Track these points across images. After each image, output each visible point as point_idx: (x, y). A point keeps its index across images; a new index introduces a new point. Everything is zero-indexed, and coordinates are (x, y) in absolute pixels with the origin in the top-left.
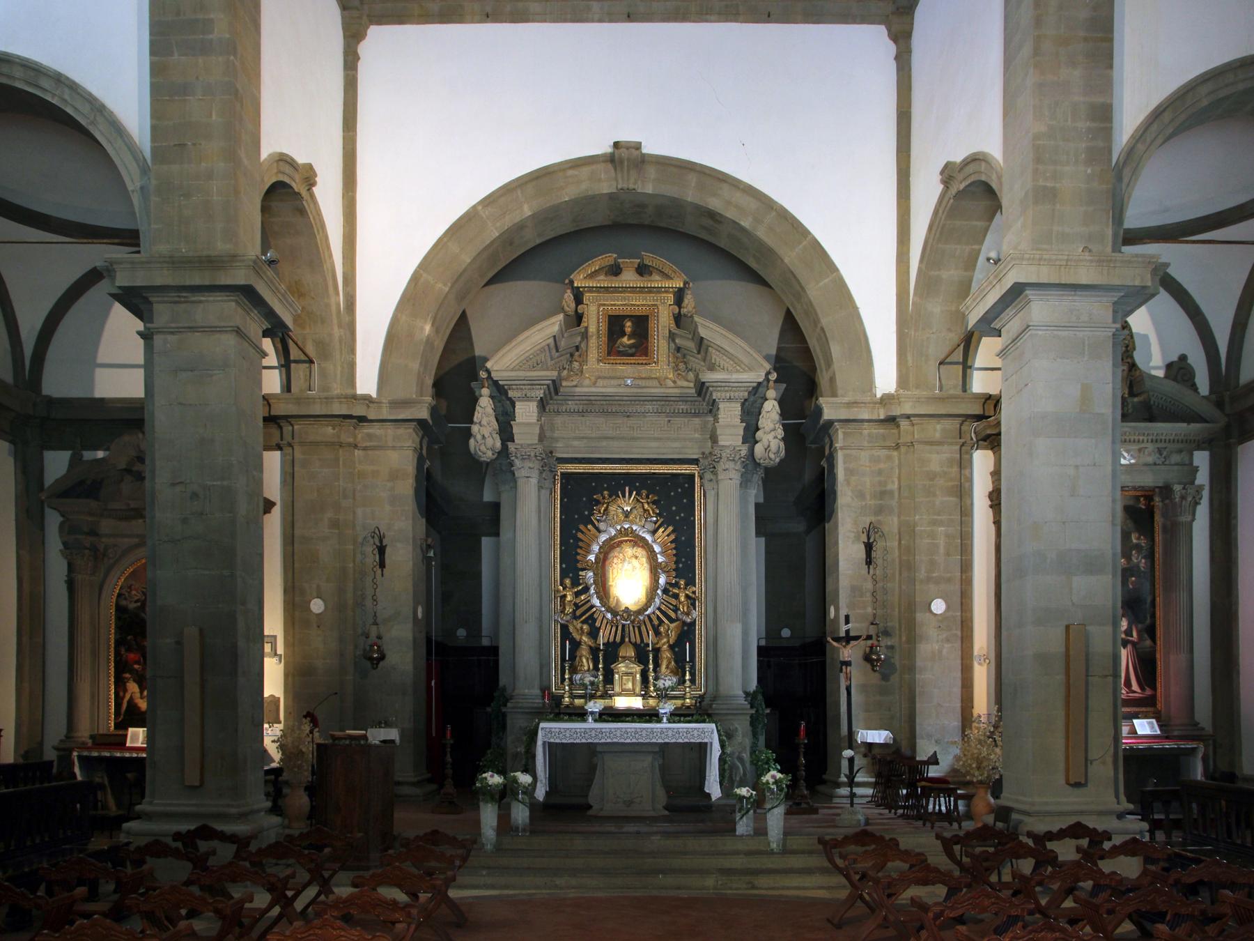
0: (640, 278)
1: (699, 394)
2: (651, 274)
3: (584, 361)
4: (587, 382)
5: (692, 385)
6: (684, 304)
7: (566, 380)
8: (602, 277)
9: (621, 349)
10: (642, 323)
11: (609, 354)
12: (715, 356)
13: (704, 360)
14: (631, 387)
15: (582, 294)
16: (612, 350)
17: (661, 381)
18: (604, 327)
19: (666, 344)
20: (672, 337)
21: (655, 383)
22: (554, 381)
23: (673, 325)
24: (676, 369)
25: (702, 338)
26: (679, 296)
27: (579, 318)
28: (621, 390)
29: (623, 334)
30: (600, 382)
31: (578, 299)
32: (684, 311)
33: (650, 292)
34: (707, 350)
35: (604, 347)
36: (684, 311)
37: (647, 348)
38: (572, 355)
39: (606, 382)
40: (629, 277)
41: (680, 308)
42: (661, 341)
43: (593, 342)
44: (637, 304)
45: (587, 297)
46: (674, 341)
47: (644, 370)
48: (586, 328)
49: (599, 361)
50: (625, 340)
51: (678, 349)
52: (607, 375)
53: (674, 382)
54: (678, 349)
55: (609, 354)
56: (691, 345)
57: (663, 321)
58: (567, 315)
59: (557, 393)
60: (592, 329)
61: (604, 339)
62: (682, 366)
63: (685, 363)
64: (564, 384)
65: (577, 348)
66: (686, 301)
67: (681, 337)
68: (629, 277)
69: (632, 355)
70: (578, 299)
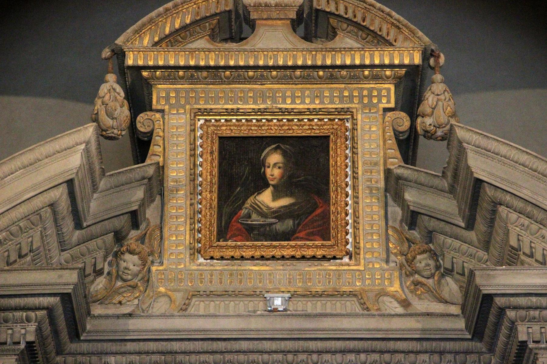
0: (306, 45)
1: (477, 332)
2: (332, 34)
3: (152, 254)
4: (161, 306)
5: (455, 310)
6: (426, 107)
7: (101, 301)
8: (202, 43)
9: (256, 220)
10: (310, 160)
11: (222, 234)
12: (517, 229)
13: (486, 245)
14: (285, 314)
15: (147, 85)
16: (231, 220)
17: (366, 302)
18: (208, 168)
19: (377, 209)
20: (394, 186)
21: (352, 305)
22: (66, 298)
23: (395, 160)
24: (408, 269)
25: (479, 182)
26: (411, 87)
27: (141, 145)
28: (255, 324)
29: (262, 184)
30: (199, 306)
31: (138, 97)
32: (425, 123)
33: (332, 79)
34: (494, 212)
35: (209, 217)
36: (425, 123)
37: (326, 217)
38: (119, 237)
39: (213, 306)
40: (274, 43)
41: (413, 115)
42: (365, 200)
43: (178, 204)
44: (299, 107)
45: (160, 93)
46: (399, 198)
47: (318, 275)
48: (161, 169)
49: (195, 252)
50: (266, 198)
51: (412, 218)
52: (216, 287)
53: (405, 304)
54: (412, 218)
55: (222, 234)
56: (447, 206)
57: (369, 144)
58: (103, 134)
59: (75, 334)
60: (177, 172)
61: (210, 196)
62: (423, 261)
63: (434, 255)
64: (97, 310)
65: (135, 218)
66: (430, 99)
67: (419, 185)
68: (274, 43)
69: (287, 236)
70: (138, 97)
